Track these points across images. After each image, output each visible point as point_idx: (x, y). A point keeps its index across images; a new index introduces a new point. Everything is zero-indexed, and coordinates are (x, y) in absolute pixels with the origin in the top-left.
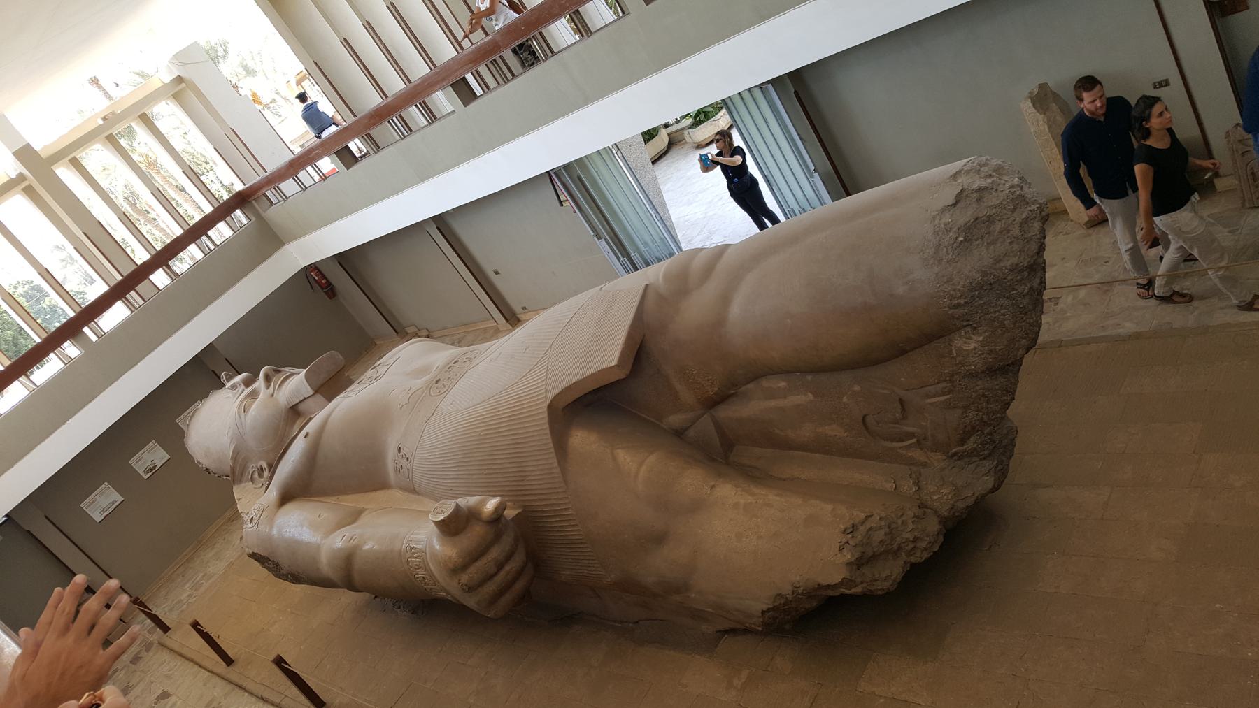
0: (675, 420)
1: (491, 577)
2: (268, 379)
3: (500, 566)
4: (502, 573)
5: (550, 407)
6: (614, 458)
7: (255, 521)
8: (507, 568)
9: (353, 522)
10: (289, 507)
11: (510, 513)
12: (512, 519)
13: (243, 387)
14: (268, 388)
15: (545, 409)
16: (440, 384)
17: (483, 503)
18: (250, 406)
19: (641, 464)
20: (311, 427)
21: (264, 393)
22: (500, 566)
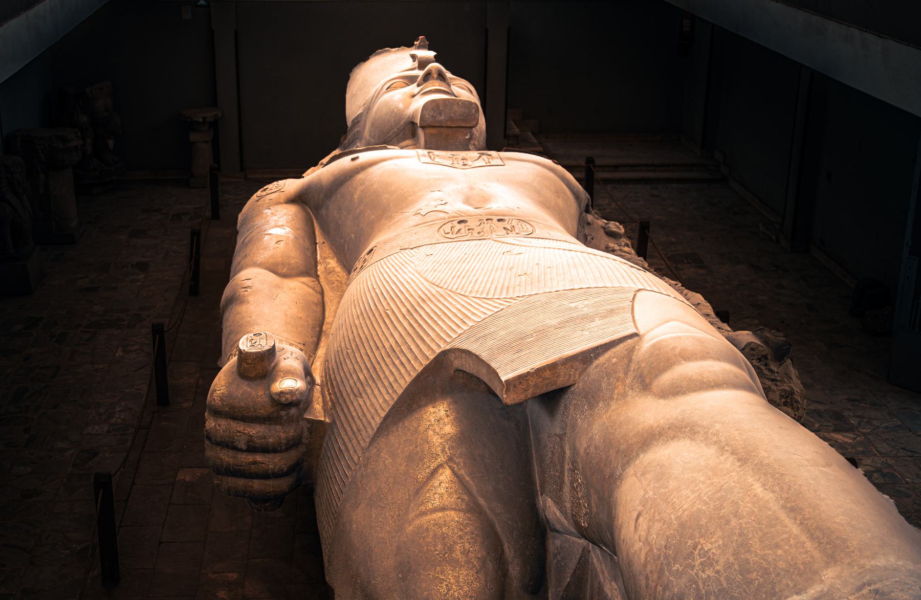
0: (550, 509)
1: (235, 449)
2: (427, 77)
3: (252, 448)
4: (250, 458)
5: (444, 353)
6: (434, 472)
7: (264, 193)
8: (259, 458)
9: (285, 276)
10: (292, 209)
11: (318, 411)
12: (309, 421)
13: (416, 64)
14: (418, 86)
15: (438, 351)
16: (458, 226)
17: (289, 373)
18: (396, 88)
19: (443, 509)
20: (365, 157)
21: (414, 88)
22: (252, 448)
